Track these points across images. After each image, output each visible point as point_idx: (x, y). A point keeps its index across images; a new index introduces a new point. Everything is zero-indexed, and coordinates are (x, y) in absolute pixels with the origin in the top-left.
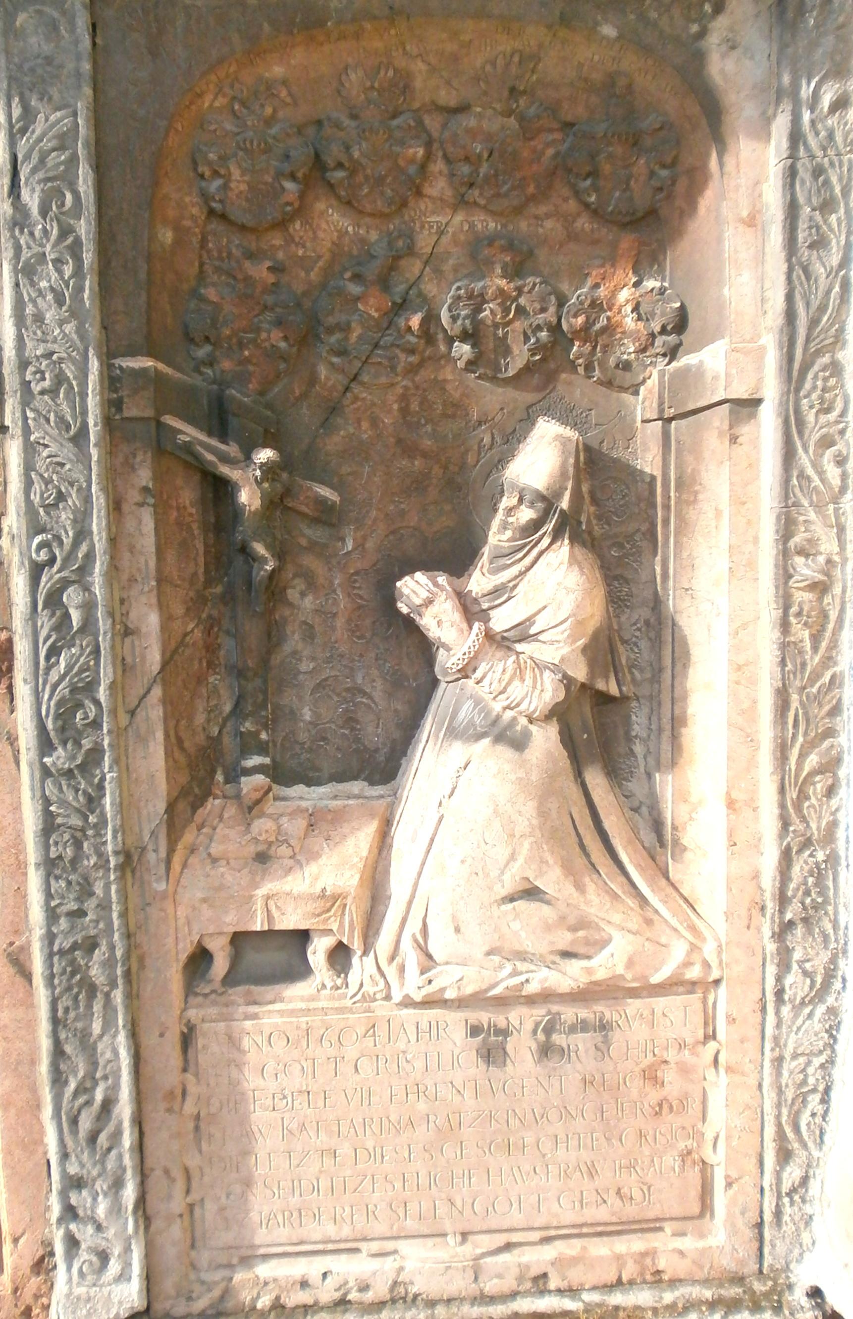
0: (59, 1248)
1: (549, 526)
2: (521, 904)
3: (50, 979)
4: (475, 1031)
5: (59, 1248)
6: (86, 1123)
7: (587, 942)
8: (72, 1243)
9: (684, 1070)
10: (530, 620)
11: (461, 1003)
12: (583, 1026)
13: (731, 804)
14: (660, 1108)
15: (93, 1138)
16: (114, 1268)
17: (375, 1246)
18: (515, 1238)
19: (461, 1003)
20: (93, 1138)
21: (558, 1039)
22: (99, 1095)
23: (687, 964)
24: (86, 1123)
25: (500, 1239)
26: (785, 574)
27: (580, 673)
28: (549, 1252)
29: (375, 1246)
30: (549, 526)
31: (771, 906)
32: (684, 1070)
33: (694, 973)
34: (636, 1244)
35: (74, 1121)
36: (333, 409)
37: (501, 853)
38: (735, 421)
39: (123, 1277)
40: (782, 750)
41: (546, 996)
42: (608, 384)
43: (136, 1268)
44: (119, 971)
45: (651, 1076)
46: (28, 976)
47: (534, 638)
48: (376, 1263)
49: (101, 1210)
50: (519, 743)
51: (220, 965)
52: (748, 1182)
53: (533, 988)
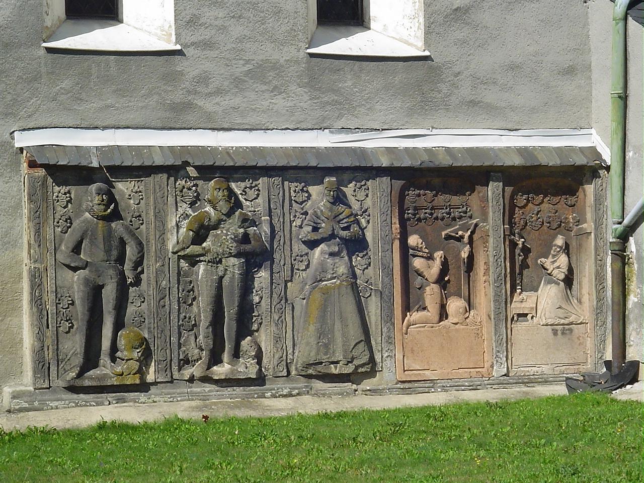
0: (495, 362)
1: (562, 251)
2: (559, 309)
3: (494, 319)
4: (553, 330)
5: (495, 362)
6: (499, 342)
7: (569, 316)
8: (497, 361)
9: (583, 338)
10: (560, 265)
11: (551, 325)
12: (569, 329)
13: (589, 294)
14: (580, 344)
15: (500, 344)
16: (503, 366)
17: (538, 366)
18: (559, 365)
19: (551, 325)
20: (500, 344)
21: (565, 331)
22: (501, 337)
23: (583, 320)
24: (499, 342)
25: (557, 365)
26: (596, 258)
27: (567, 273)
28: (564, 367)
29: (538, 366)
30: (562, 251)
31: (596, 310)
32: (583, 338)
33: (585, 321)
34: (577, 367)
35: (498, 341)
36: (529, 233)
37: (556, 301)
38: (588, 235)
39: (504, 368)
40: (596, 285)
41: (563, 324)
42: (568, 230)
43: (506, 366)
44: (504, 318)
45: (578, 338)
46: (490, 319)
47: (560, 268)
48: (538, 369)
49: (501, 356)
50: (559, 284)
51: (515, 318)
52: (594, 356)
53: (562, 323)
